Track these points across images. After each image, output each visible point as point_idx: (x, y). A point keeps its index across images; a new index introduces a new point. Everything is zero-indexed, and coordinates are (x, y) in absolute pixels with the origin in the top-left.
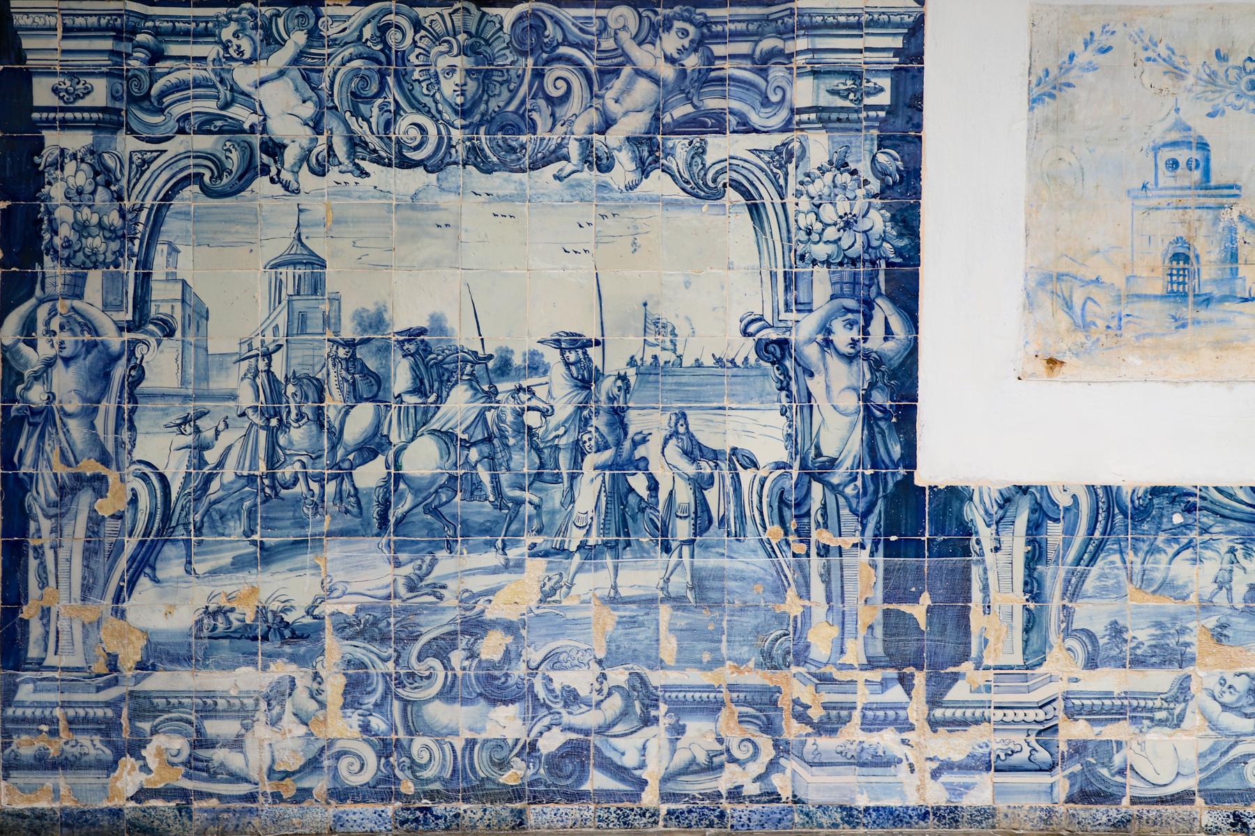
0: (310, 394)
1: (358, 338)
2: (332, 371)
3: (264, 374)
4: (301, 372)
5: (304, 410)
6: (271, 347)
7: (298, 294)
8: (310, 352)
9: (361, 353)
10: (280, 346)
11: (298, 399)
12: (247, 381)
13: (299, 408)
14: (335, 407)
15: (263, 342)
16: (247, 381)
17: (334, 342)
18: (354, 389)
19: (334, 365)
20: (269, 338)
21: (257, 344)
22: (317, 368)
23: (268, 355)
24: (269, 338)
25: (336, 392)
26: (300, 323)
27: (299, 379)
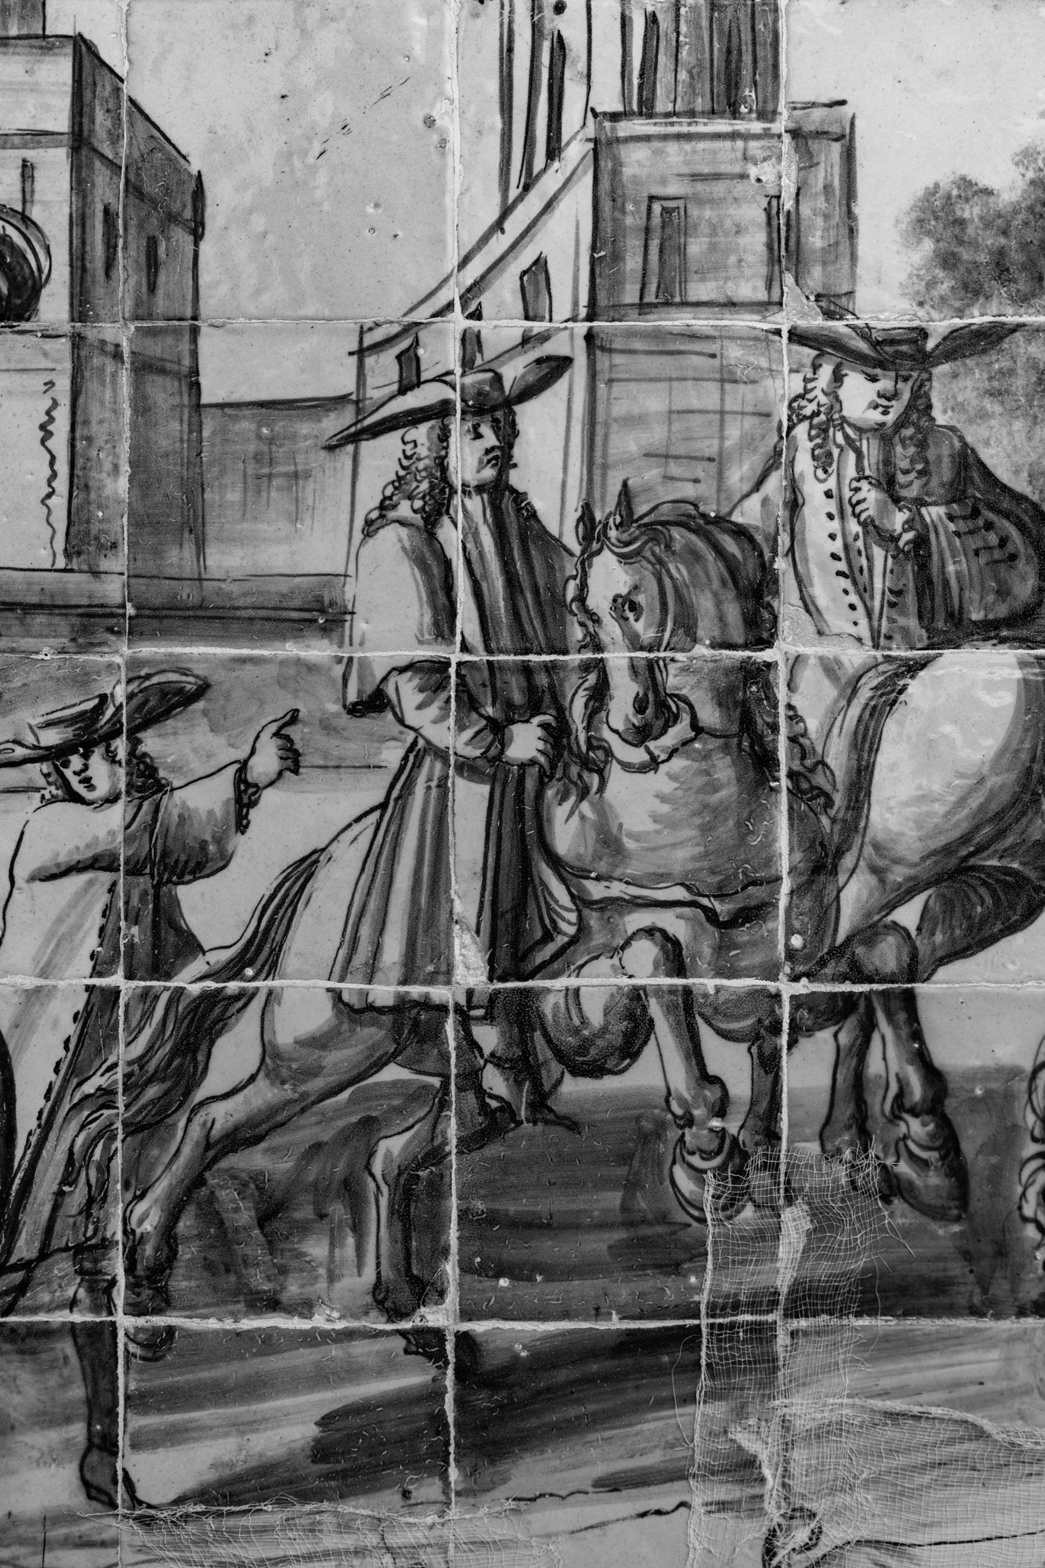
0: (704, 604)
1: (941, 326)
2: (813, 491)
3: (475, 504)
4: (658, 490)
5: (673, 681)
6: (513, 372)
7: (646, 109)
8: (708, 396)
9: (955, 395)
10: (556, 367)
11: (644, 628)
12: (391, 540)
13: (649, 674)
14: (830, 668)
15: (471, 342)
16: (391, 540)
17: (820, 343)
18: (925, 584)
19: (823, 461)
20: (502, 325)
21: (441, 351)
22: (738, 476)
23: (496, 409)
24: (502, 325)
25: (828, 589)
26: (644, 255)
27: (655, 530)
